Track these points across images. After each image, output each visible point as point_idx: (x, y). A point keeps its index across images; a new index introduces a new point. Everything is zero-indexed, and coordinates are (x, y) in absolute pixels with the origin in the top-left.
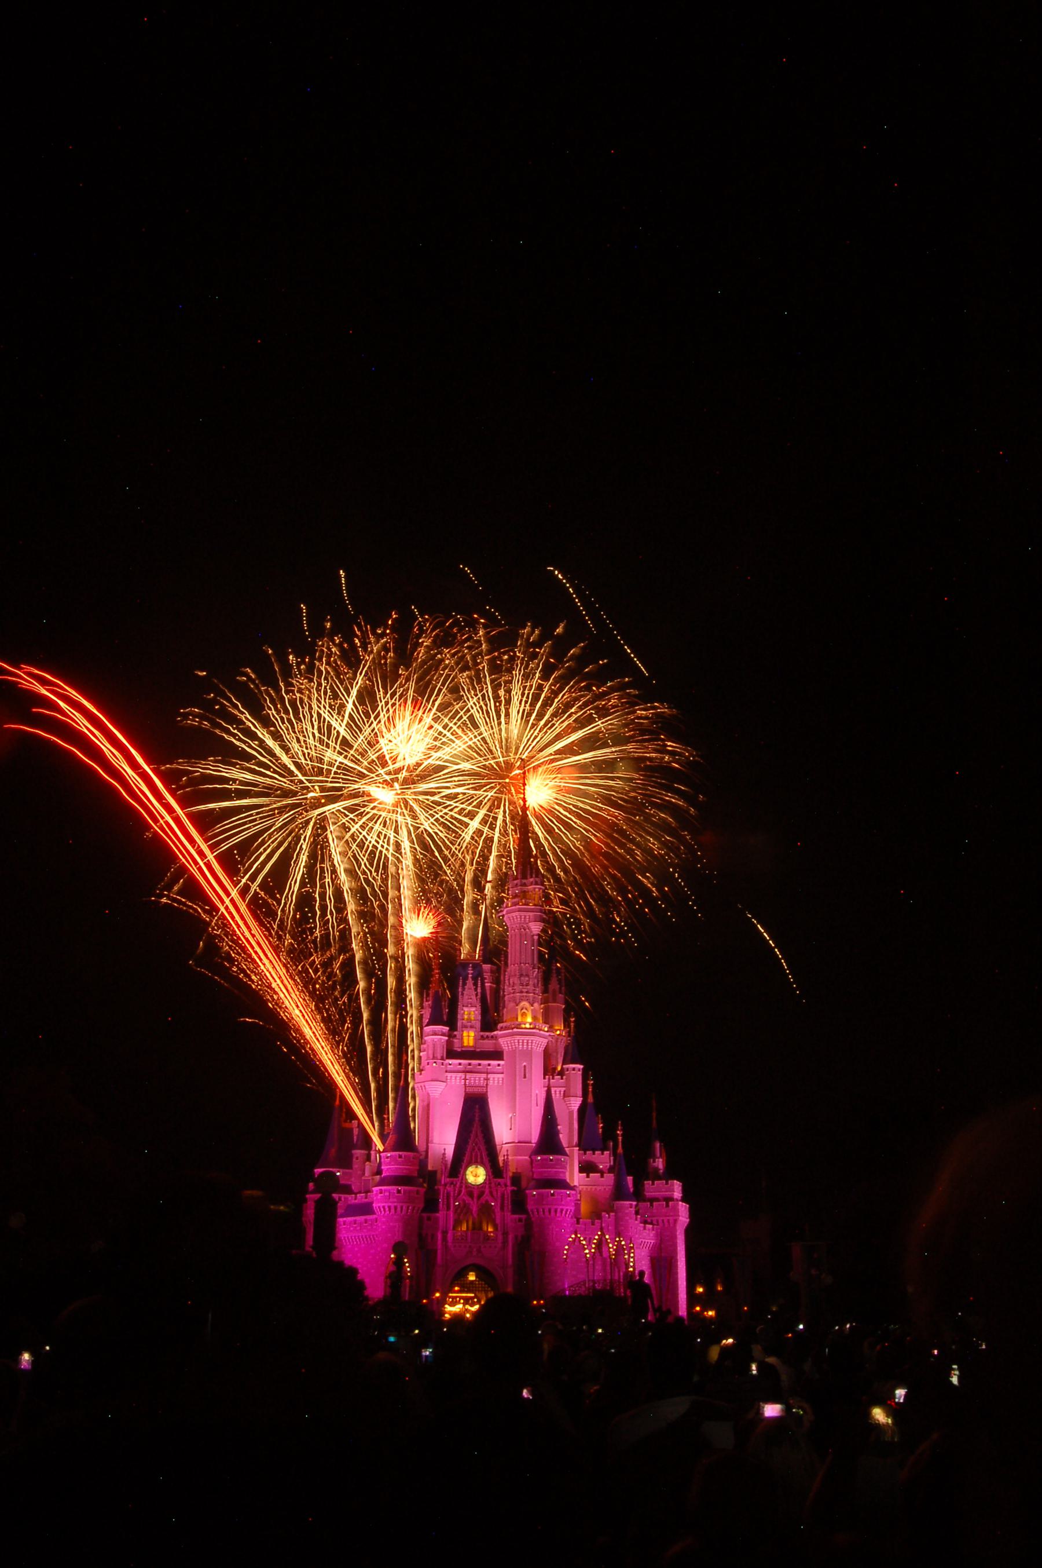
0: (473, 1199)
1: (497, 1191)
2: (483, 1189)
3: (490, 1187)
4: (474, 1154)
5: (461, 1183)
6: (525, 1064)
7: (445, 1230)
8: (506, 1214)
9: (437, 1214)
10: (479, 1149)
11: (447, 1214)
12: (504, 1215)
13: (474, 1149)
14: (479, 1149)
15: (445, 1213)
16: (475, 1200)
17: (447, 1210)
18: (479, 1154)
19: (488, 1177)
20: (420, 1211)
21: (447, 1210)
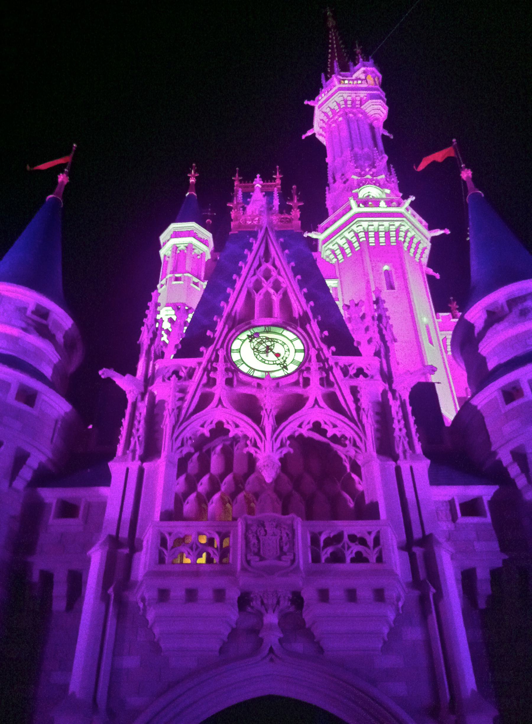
0: (257, 419)
1: (354, 391)
2: (299, 390)
3: (326, 382)
4: (258, 298)
5: (209, 369)
6: (386, 267)
7: (124, 534)
8: (405, 465)
9: (103, 490)
10: (277, 287)
11: (141, 471)
12: (398, 470)
13: (258, 287)
14: (277, 287)
15: (134, 466)
16: (268, 423)
17: (143, 459)
18: (276, 298)
19: (313, 353)
20: (26, 474)
21: (143, 459)
